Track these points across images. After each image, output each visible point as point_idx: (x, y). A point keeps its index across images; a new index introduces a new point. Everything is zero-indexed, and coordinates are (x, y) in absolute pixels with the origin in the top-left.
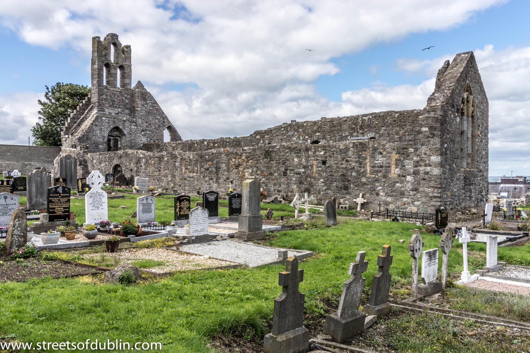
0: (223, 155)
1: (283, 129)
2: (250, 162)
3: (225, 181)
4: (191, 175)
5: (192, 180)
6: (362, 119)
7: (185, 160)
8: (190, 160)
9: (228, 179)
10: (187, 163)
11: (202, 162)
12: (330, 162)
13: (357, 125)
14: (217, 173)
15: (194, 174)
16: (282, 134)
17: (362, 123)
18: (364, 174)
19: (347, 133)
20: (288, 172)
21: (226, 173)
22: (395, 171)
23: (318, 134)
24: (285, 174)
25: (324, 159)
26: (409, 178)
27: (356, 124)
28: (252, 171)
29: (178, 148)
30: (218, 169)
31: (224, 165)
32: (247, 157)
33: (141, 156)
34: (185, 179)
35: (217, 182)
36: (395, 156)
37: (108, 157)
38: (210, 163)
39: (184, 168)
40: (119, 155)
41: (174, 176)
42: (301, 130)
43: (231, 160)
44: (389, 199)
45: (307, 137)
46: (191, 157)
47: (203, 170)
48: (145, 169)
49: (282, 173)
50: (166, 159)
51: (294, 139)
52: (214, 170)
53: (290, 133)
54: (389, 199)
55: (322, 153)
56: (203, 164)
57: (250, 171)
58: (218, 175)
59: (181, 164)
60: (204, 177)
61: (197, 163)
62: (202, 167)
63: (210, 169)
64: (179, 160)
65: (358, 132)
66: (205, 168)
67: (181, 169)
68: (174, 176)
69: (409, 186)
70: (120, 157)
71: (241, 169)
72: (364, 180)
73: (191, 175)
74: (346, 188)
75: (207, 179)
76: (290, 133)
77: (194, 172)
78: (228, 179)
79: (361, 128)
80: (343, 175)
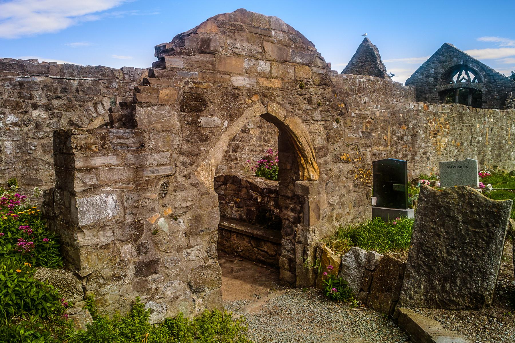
0: (421, 114)
2: (448, 126)
6: (359, 80)
7: (366, 118)
8: (376, 119)
10: (369, 126)
12: (495, 130)
13: (356, 87)
14: (413, 143)
15: (381, 148)
17: (360, 85)
20: (473, 141)
21: (423, 144)
24: (471, 142)
25: (491, 126)
27: (354, 84)
28: (448, 141)
30: (414, 136)
31: (421, 132)
32: (446, 120)
37: (45, 87)
38: (406, 127)
43: (431, 123)
46: (378, 114)
48: (260, 139)
49: (469, 143)
55: (492, 120)
56: (395, 128)
57: (447, 139)
58: (414, 147)
62: (394, 133)
65: (356, 95)
66: (399, 137)
79: (359, 90)
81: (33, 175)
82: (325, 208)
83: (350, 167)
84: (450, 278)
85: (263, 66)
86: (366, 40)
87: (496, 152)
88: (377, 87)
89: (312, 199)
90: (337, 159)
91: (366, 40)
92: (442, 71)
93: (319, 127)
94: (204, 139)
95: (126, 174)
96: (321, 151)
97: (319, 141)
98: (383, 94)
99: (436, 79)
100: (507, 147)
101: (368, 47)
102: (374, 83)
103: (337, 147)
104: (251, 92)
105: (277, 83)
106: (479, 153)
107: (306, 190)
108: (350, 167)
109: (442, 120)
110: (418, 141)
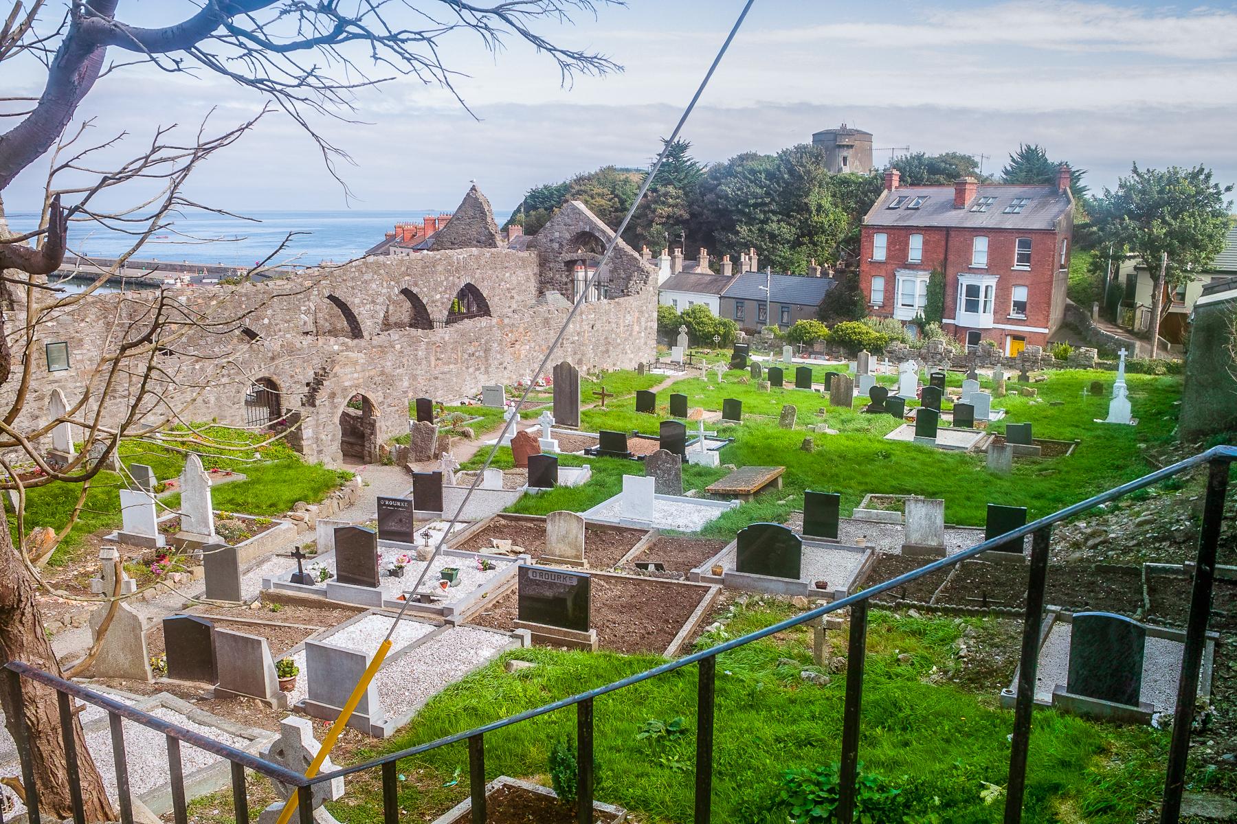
1: (353, 269)
3: (497, 368)
4: (446, 369)
5: (448, 376)
8: (445, 343)
9: (501, 364)
10: (438, 349)
11: (463, 344)
12: (598, 326)
15: (452, 366)
16: (353, 278)
18: (618, 335)
19: (443, 278)
21: (499, 356)
22: (636, 328)
23: (407, 278)
25: (592, 323)
26: (643, 334)
29: (86, 316)
30: (487, 351)
31: (496, 345)
32: (525, 329)
33: (336, 347)
34: (436, 378)
35: (487, 372)
36: (637, 314)
38: (477, 344)
39: (433, 359)
40: (270, 354)
41: (414, 377)
42: (382, 271)
44: (632, 356)
45: (392, 283)
46: (447, 338)
47: (466, 356)
50: (397, 347)
51: (374, 286)
52: (482, 353)
53: (366, 277)
54: (632, 356)
58: (487, 360)
59: (428, 353)
60: (467, 368)
61: (457, 347)
63: (477, 354)
64: (424, 347)
67: (429, 362)
68: (414, 377)
69: (643, 341)
70: (273, 359)
71: (517, 346)
72: (619, 341)
73: (446, 369)
74: (607, 351)
75: (471, 370)
76: (366, 277)
77: (449, 363)
78: (501, 364)
79: (457, 270)
80: (606, 338)
81: (223, 413)
82: (384, 428)
83: (397, 408)
84: (421, 452)
85: (356, 375)
86: (473, 188)
87: (602, 348)
88: (482, 262)
89: (377, 425)
90: (390, 406)
91: (473, 188)
92: (568, 236)
93: (380, 393)
94: (336, 407)
95: (314, 422)
96: (382, 403)
97: (380, 399)
98: (491, 269)
99: (561, 245)
100: (619, 341)
101: (476, 199)
102: (478, 258)
103: (389, 400)
104: (351, 387)
105: (361, 380)
106: (575, 353)
107: (375, 421)
108: (397, 408)
109: (521, 330)
110: (493, 353)
